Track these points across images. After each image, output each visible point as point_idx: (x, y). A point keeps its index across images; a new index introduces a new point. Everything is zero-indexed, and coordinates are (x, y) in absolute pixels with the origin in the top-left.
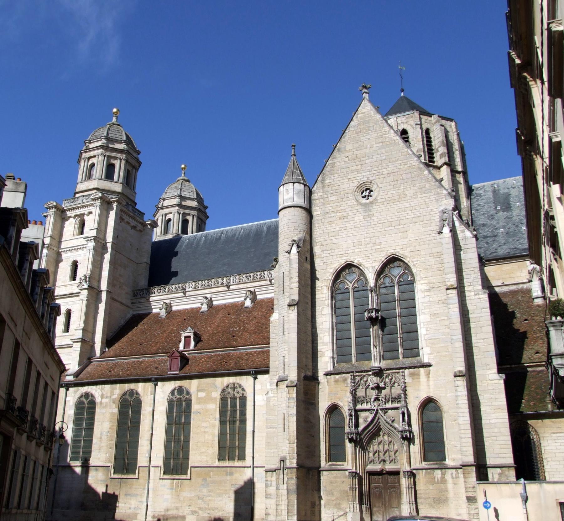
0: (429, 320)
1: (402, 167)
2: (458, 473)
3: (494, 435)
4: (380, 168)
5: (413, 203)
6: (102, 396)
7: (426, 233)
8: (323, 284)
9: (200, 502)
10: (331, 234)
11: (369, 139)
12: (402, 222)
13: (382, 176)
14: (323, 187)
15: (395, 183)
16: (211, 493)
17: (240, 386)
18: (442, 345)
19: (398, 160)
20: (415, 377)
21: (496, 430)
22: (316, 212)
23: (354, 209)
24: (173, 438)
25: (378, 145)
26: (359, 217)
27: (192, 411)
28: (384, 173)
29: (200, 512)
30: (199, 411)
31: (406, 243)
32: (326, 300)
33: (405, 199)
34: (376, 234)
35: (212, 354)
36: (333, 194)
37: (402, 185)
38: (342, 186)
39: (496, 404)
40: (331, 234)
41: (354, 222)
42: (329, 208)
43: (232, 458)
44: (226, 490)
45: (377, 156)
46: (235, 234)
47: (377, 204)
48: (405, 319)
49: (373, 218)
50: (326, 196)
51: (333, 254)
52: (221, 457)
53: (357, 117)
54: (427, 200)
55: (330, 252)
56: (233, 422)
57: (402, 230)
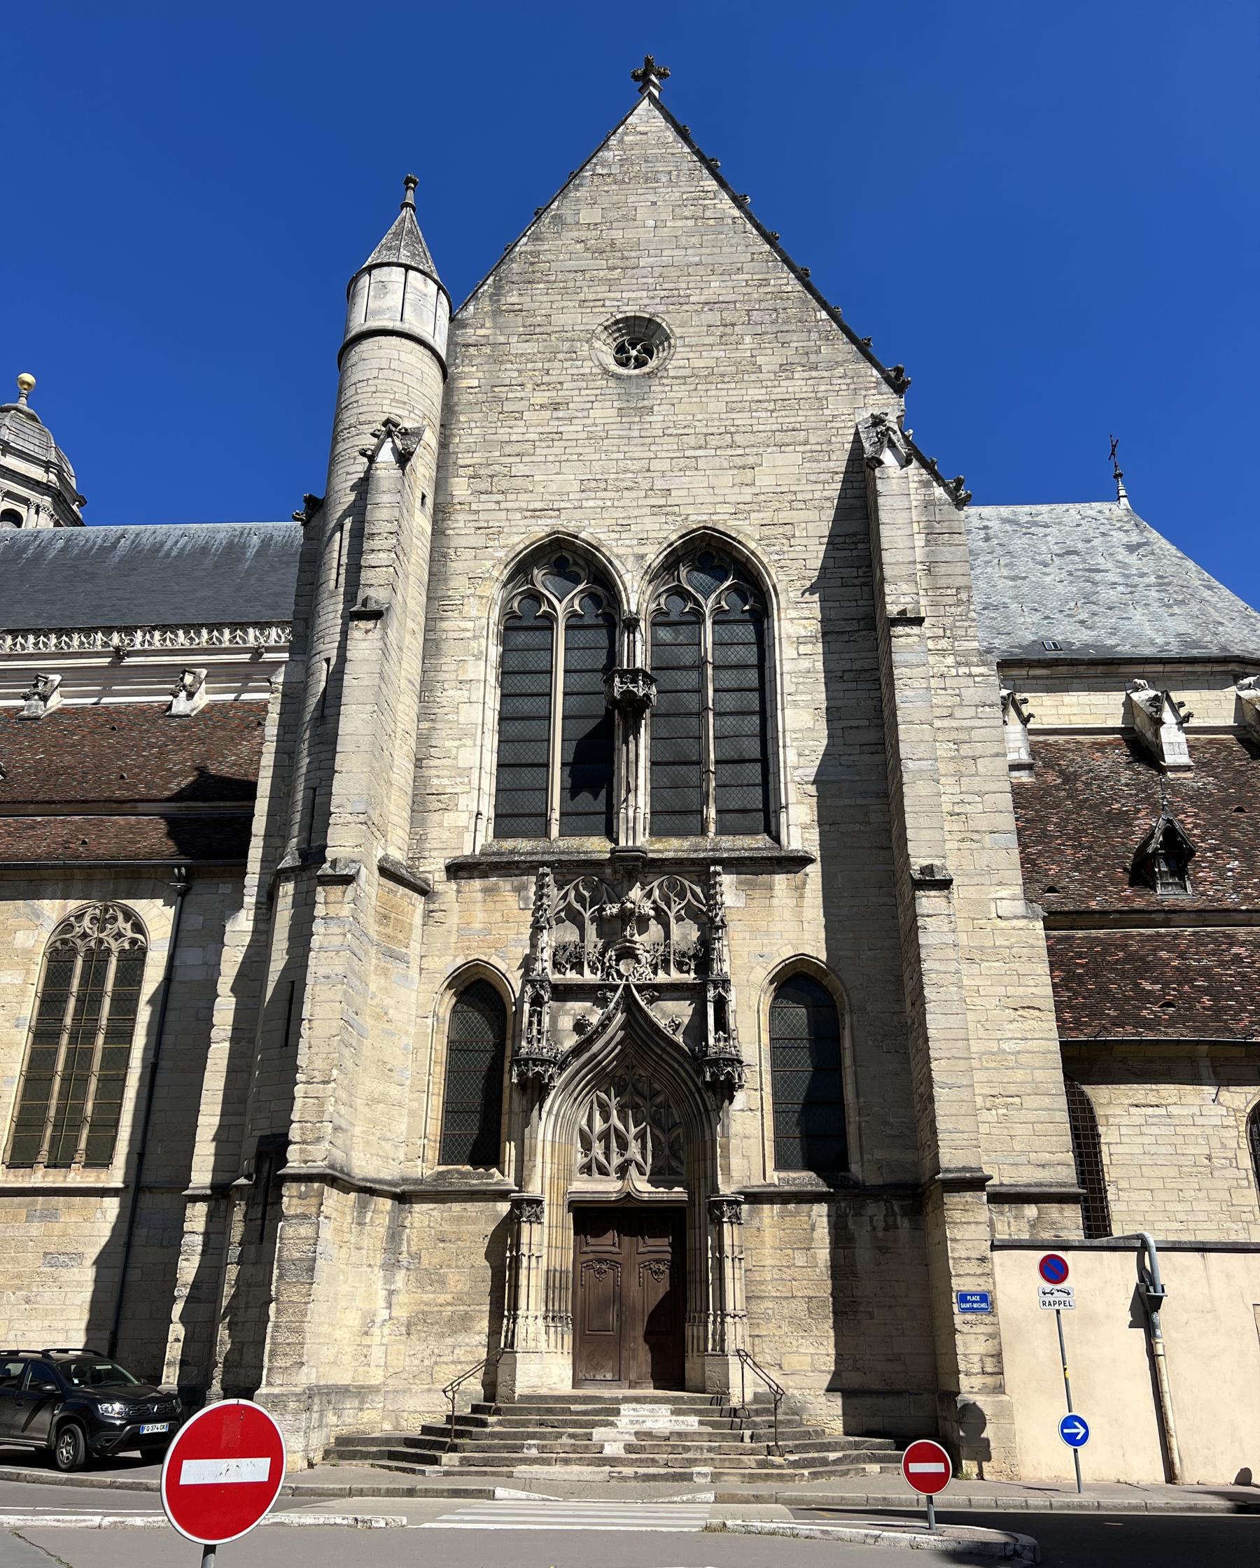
0: (811, 725)
1: (749, 290)
2: (894, 1214)
3: (1012, 1089)
4: (684, 285)
5: (778, 393)
7: (813, 478)
8: (469, 592)
10: (508, 450)
11: (654, 203)
12: (738, 439)
13: (685, 307)
14: (497, 313)
15: (729, 330)
17: (128, 915)
18: (848, 802)
19: (740, 270)
20: (757, 893)
21: (1020, 1075)
22: (471, 378)
23: (591, 385)
25: (679, 223)
26: (604, 413)
28: (692, 299)
31: (748, 498)
32: (475, 637)
33: (754, 377)
34: (655, 465)
35: (39, 819)
36: (528, 336)
37: (748, 339)
38: (559, 319)
39: (1021, 991)
40: (508, 450)
41: (588, 421)
42: (510, 373)
43: (60, 1161)
45: (676, 252)
47: (665, 381)
48: (729, 721)
49: (648, 419)
50: (502, 339)
51: (510, 505)
53: (621, 141)
54: (823, 388)
55: (500, 497)
56: (83, 1035)
57: (738, 461)
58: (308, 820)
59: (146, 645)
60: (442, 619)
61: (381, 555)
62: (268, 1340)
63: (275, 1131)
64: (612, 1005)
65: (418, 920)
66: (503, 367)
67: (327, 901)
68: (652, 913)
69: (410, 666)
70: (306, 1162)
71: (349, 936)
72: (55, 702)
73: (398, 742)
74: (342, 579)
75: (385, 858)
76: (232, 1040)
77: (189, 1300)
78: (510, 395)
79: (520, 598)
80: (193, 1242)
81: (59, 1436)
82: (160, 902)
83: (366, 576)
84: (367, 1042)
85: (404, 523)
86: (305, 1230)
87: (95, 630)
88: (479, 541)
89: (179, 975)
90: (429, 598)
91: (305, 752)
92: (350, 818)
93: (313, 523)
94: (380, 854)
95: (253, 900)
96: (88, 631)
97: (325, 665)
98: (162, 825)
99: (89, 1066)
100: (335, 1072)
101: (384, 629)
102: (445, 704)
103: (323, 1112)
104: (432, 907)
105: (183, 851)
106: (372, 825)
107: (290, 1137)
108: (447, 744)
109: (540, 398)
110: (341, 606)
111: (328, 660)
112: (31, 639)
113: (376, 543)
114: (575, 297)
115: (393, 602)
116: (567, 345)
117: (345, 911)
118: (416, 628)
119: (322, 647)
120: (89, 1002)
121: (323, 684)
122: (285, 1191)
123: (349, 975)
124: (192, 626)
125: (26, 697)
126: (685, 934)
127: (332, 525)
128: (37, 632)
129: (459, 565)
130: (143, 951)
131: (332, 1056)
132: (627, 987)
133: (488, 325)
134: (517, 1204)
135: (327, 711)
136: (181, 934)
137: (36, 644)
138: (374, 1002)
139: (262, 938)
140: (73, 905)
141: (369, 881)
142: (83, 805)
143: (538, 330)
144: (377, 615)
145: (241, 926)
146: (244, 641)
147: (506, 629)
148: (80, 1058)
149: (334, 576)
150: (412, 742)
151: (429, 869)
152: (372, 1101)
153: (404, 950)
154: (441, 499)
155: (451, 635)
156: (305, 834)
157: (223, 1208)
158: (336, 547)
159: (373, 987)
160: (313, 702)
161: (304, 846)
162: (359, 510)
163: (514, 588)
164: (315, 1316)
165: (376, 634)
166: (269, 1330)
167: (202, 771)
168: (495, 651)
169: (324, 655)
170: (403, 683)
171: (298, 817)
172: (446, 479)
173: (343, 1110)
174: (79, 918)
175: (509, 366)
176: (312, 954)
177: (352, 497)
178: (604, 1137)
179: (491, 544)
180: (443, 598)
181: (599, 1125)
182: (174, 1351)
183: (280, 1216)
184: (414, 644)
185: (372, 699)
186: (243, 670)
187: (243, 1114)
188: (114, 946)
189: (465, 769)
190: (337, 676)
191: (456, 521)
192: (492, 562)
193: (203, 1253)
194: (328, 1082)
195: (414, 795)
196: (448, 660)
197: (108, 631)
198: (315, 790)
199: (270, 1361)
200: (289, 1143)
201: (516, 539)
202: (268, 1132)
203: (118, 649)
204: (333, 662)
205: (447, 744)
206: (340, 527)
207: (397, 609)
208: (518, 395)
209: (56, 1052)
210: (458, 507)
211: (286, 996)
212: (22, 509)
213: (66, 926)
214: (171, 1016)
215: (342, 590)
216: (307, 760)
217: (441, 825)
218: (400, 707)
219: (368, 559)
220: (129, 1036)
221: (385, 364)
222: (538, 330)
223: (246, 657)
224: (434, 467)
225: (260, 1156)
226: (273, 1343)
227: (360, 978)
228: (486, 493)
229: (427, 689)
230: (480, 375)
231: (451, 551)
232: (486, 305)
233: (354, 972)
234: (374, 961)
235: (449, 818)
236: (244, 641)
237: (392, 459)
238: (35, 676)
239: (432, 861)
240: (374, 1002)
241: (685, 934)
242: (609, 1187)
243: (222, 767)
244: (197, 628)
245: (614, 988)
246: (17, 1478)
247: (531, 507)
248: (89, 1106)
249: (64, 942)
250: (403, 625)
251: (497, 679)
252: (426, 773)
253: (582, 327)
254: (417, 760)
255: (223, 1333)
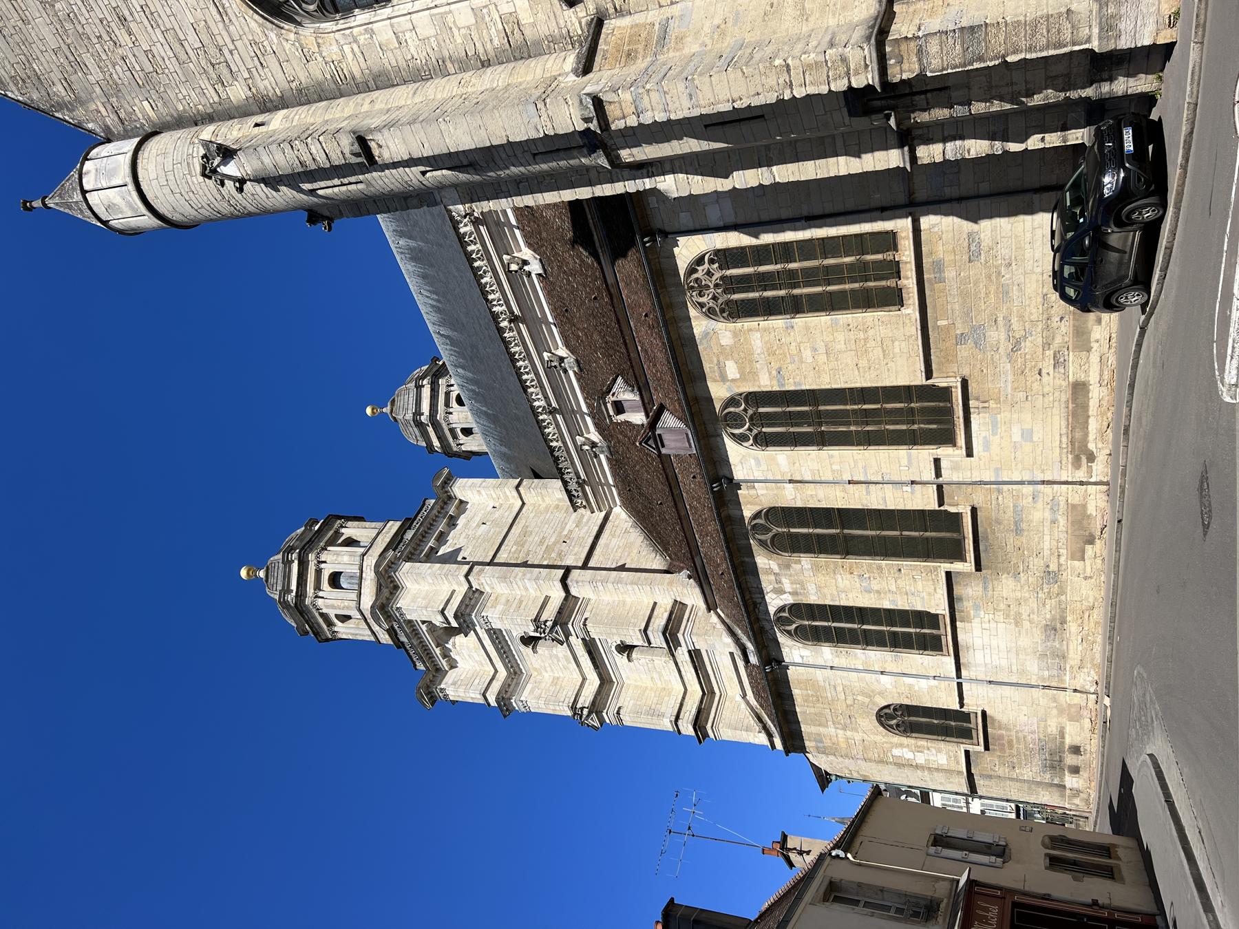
6: (780, 591)
9: (1027, 346)
10: (183, 57)
16: (1000, 319)
17: (691, 270)
22: (145, 110)
24: (853, 428)
27: (776, 388)
29: (1058, 340)
30: (774, 373)
32: (356, 41)
36: (82, 65)
43: (894, 269)
44: (989, 277)
46: (433, 306)
50: (98, 90)
52: (894, 299)
55: (226, 52)
56: (791, 279)
58: (562, 154)
59: (501, 302)
60: (354, 78)
61: (314, 151)
62: (1044, 54)
63: (842, 103)
65: (626, 21)
66: (119, 82)
67: (622, 117)
69: (401, 98)
70: (866, 66)
71: (648, 87)
72: (562, 352)
73: (470, 90)
74: (353, 179)
75: (575, 72)
76: (769, 165)
77: (1006, 139)
78: (138, 68)
79: (304, 5)
80: (952, 150)
81: (1132, 223)
82: (676, 250)
83: (337, 160)
84: (749, 38)
85: (281, 137)
86: (933, 47)
87: (503, 339)
88: (271, 61)
89: (731, 220)
90: (342, 96)
91: (507, 172)
92: (544, 117)
93: (327, 214)
94: (572, 77)
95: (647, 180)
96: (506, 344)
97: (428, 175)
98: (620, 262)
99: (817, 268)
100: (777, 62)
101: (371, 131)
102: (424, 53)
103: (816, 63)
104: (612, 11)
105: (632, 244)
106: (547, 91)
107: (845, 88)
108: (459, 41)
109: (124, 38)
110: (374, 174)
111: (424, 173)
112: (525, 377)
113: (306, 158)
114: (24, 30)
115: (349, 128)
116: (68, 26)
117: (626, 96)
118: (368, 100)
119: (414, 181)
120: (765, 281)
121: (445, 172)
122: (896, 80)
123: (684, 75)
124: (475, 275)
125: (565, 371)
127: (316, 200)
128: (519, 375)
129: (303, 74)
130: (717, 252)
131: (763, 70)
133: (94, 107)
135: (465, 163)
136: (698, 227)
137: (528, 373)
138: (708, 41)
139: (677, 164)
140: (693, 312)
141: (595, 83)
142: (621, 322)
143: (72, 59)
144: (362, 141)
145: (671, 185)
146: (471, 234)
147: (337, 11)
148: (810, 277)
149: (353, 187)
150: (467, 75)
151: (577, 24)
152: (804, 15)
153: (657, 26)
154: (255, 108)
155: (363, 66)
156: (575, 153)
157: (919, 132)
158: (329, 191)
159: (695, 48)
160: (463, 177)
161: (585, 150)
162: (292, 180)
163: (298, 14)
164: (1019, 11)
165: (378, 137)
166: (1034, 56)
167: (574, 242)
168: (361, 17)
169: (421, 178)
170: (418, 99)
171: (563, 163)
172: (237, 108)
173: (813, 43)
174: (702, 305)
175: (115, 76)
176: (673, 117)
177: (283, 188)
179: (269, 49)
180: (336, 82)
182: (1053, 140)
183: (921, 77)
184: (382, 99)
185: (435, 125)
186: (494, 229)
187: (833, 137)
188: (717, 275)
189: (475, 14)
190: (433, 162)
191: (266, 88)
192: (284, 43)
193: (962, 138)
194: (788, 66)
195: (516, 60)
196: (385, 61)
197: (501, 331)
198: (535, 155)
199: (1065, 46)
200: (850, 88)
201: (253, 25)
202: (845, 110)
203: (510, 322)
204: (422, 168)
205: (459, 41)
206: (312, 192)
207: (354, 123)
208: (133, 60)
209: (809, 296)
210: (254, 90)
211: (718, 131)
212: (454, 395)
213: (710, 313)
214: (765, 217)
215: (361, 177)
216: (512, 168)
217: (534, 25)
218: (439, 96)
219: (322, 161)
220: (786, 246)
221: (166, 190)
222: (72, 59)
223: (483, 229)
224: (230, 122)
225: (868, 112)
226: (1048, 47)
227: (687, 64)
228: (229, 66)
229: (418, 75)
230: (137, 101)
231: (293, 85)
232: (80, 113)
233: (681, 72)
234: (671, 54)
235: (526, 18)
236: (471, 234)
237: (232, 163)
238: (549, 369)
239: (569, 24)
240: (708, 41)
243: (565, 226)
244: (475, 271)
246: (1169, 249)
247: (218, 17)
248: (848, 260)
249: (722, 311)
250: (368, 114)
251: (384, 7)
252: (492, 54)
253: (45, 15)
254: (483, 66)
255: (1037, 100)
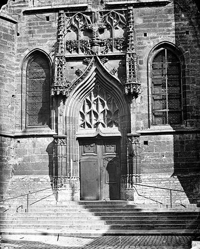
64: (89, 65)
68: (105, 27)
126: (119, 33)
132: (95, 57)
134: (56, 138)
178: (90, 113)
181: (87, 110)
241: (119, 33)
242: (90, 133)
245: (91, 58)
